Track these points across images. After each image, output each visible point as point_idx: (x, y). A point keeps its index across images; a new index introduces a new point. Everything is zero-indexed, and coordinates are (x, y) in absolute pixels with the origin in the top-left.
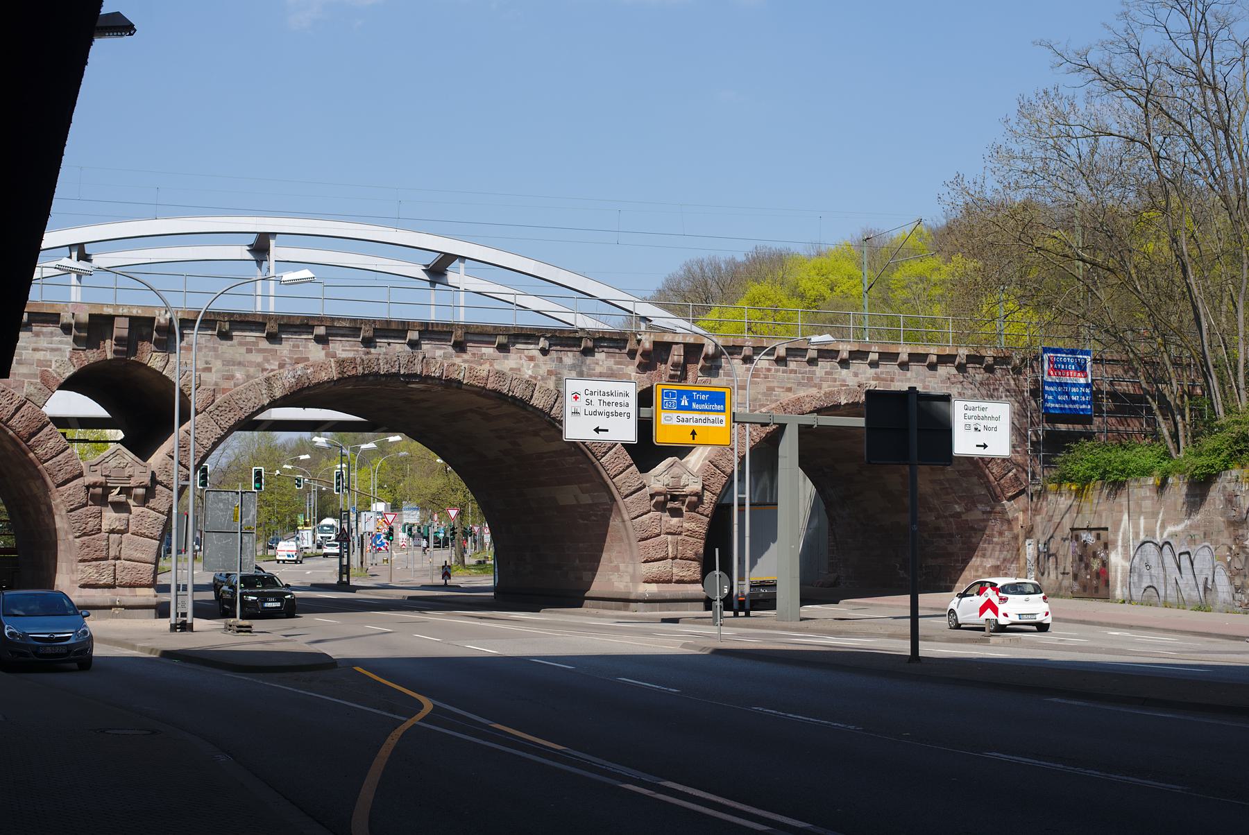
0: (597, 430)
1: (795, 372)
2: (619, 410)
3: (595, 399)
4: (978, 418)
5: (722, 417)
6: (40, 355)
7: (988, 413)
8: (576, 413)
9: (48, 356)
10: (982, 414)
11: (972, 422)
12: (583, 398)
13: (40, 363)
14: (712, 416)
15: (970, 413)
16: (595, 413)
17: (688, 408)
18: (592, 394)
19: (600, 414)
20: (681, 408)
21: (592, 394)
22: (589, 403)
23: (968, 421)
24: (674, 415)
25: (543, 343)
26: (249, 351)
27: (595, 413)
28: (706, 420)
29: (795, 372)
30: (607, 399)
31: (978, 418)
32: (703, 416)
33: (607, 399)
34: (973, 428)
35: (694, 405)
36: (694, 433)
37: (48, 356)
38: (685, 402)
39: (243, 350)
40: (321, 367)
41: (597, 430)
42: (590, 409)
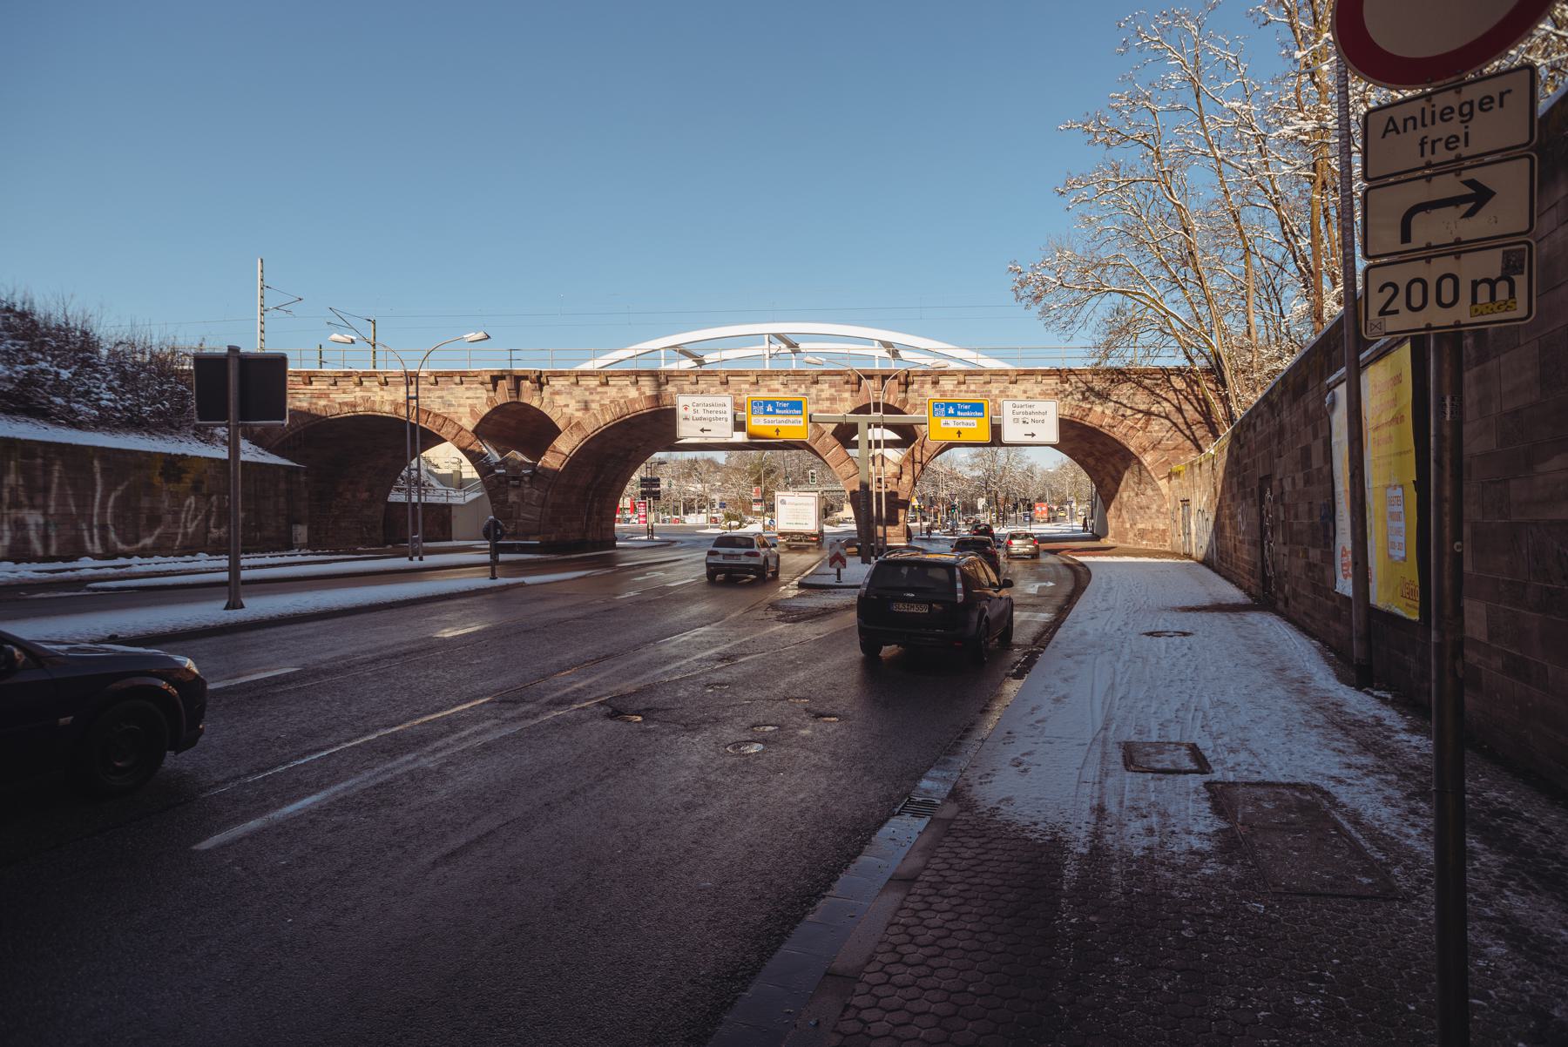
0: (702, 430)
1: (975, 392)
2: (719, 416)
3: (700, 409)
4: (1026, 413)
5: (801, 418)
6: (470, 401)
7: (1035, 410)
8: (686, 419)
9: (475, 401)
10: (1029, 410)
11: (1021, 416)
12: (691, 409)
13: (470, 405)
14: (792, 418)
15: (1017, 410)
16: (700, 419)
17: (773, 413)
18: (698, 405)
19: (705, 419)
20: (766, 413)
21: (698, 405)
22: (696, 412)
23: (1016, 416)
24: (762, 418)
25: (457, 379)
26: (591, 393)
27: (700, 419)
28: (786, 422)
29: (975, 392)
30: (709, 409)
31: (1026, 413)
32: (785, 419)
33: (709, 409)
34: (1021, 421)
35: (777, 411)
36: (777, 431)
37: (475, 401)
38: (770, 409)
39: (587, 393)
40: (633, 401)
41: (702, 430)
42: (697, 416)
